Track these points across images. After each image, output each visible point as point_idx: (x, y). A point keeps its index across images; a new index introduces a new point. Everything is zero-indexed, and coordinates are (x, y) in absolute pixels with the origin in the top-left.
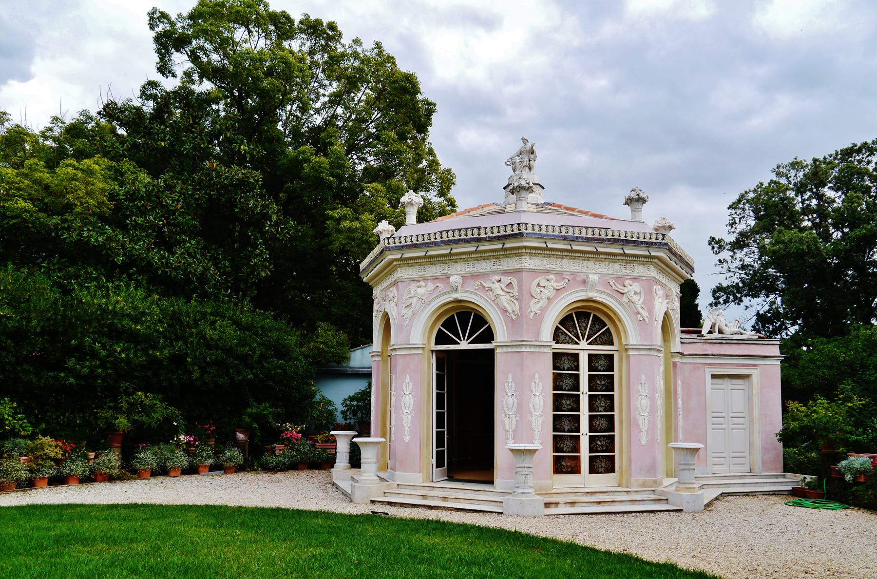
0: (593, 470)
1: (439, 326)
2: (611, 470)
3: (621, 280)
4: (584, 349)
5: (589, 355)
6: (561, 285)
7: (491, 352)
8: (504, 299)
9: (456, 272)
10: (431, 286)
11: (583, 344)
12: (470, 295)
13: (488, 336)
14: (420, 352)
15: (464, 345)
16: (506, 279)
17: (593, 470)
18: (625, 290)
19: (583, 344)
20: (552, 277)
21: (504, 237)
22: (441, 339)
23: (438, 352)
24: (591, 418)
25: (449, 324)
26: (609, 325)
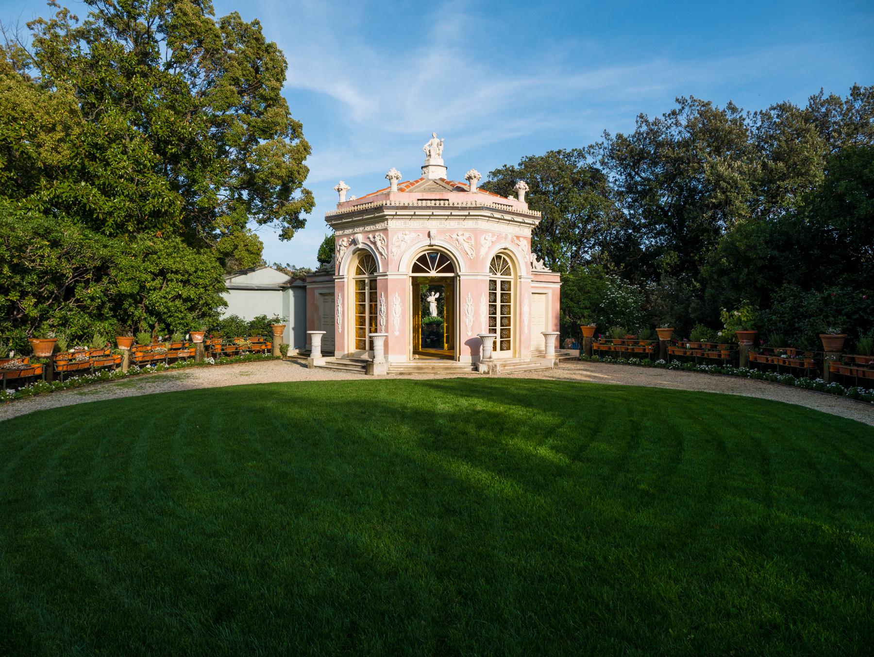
0: (502, 349)
1: (415, 260)
2: (509, 348)
3: (518, 237)
4: (499, 278)
5: (502, 282)
6: (494, 239)
7: (453, 279)
8: (466, 245)
9: (433, 225)
10: (413, 235)
11: (499, 275)
12: (439, 242)
13: (450, 268)
14: (405, 277)
15: (433, 273)
16: (467, 235)
17: (502, 349)
18: (520, 243)
19: (499, 275)
20: (490, 234)
21: (470, 208)
22: (416, 269)
23: (413, 277)
24: (502, 318)
25: (422, 259)
26: (510, 264)
